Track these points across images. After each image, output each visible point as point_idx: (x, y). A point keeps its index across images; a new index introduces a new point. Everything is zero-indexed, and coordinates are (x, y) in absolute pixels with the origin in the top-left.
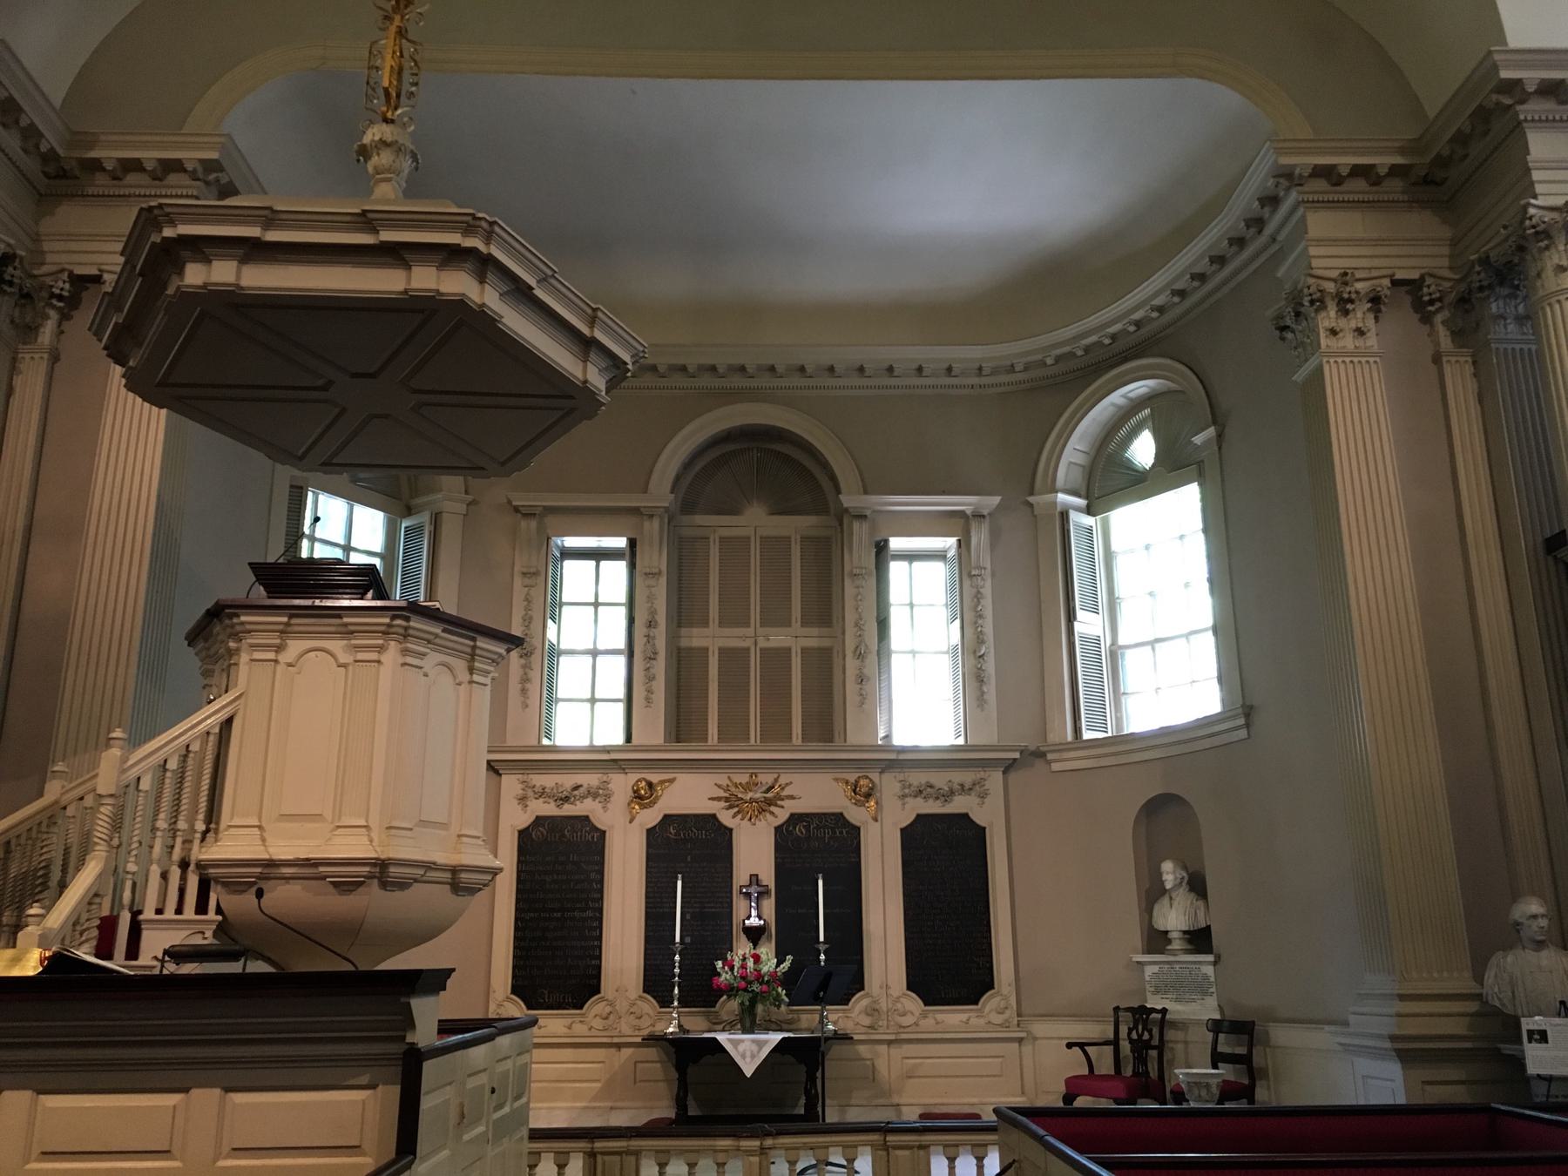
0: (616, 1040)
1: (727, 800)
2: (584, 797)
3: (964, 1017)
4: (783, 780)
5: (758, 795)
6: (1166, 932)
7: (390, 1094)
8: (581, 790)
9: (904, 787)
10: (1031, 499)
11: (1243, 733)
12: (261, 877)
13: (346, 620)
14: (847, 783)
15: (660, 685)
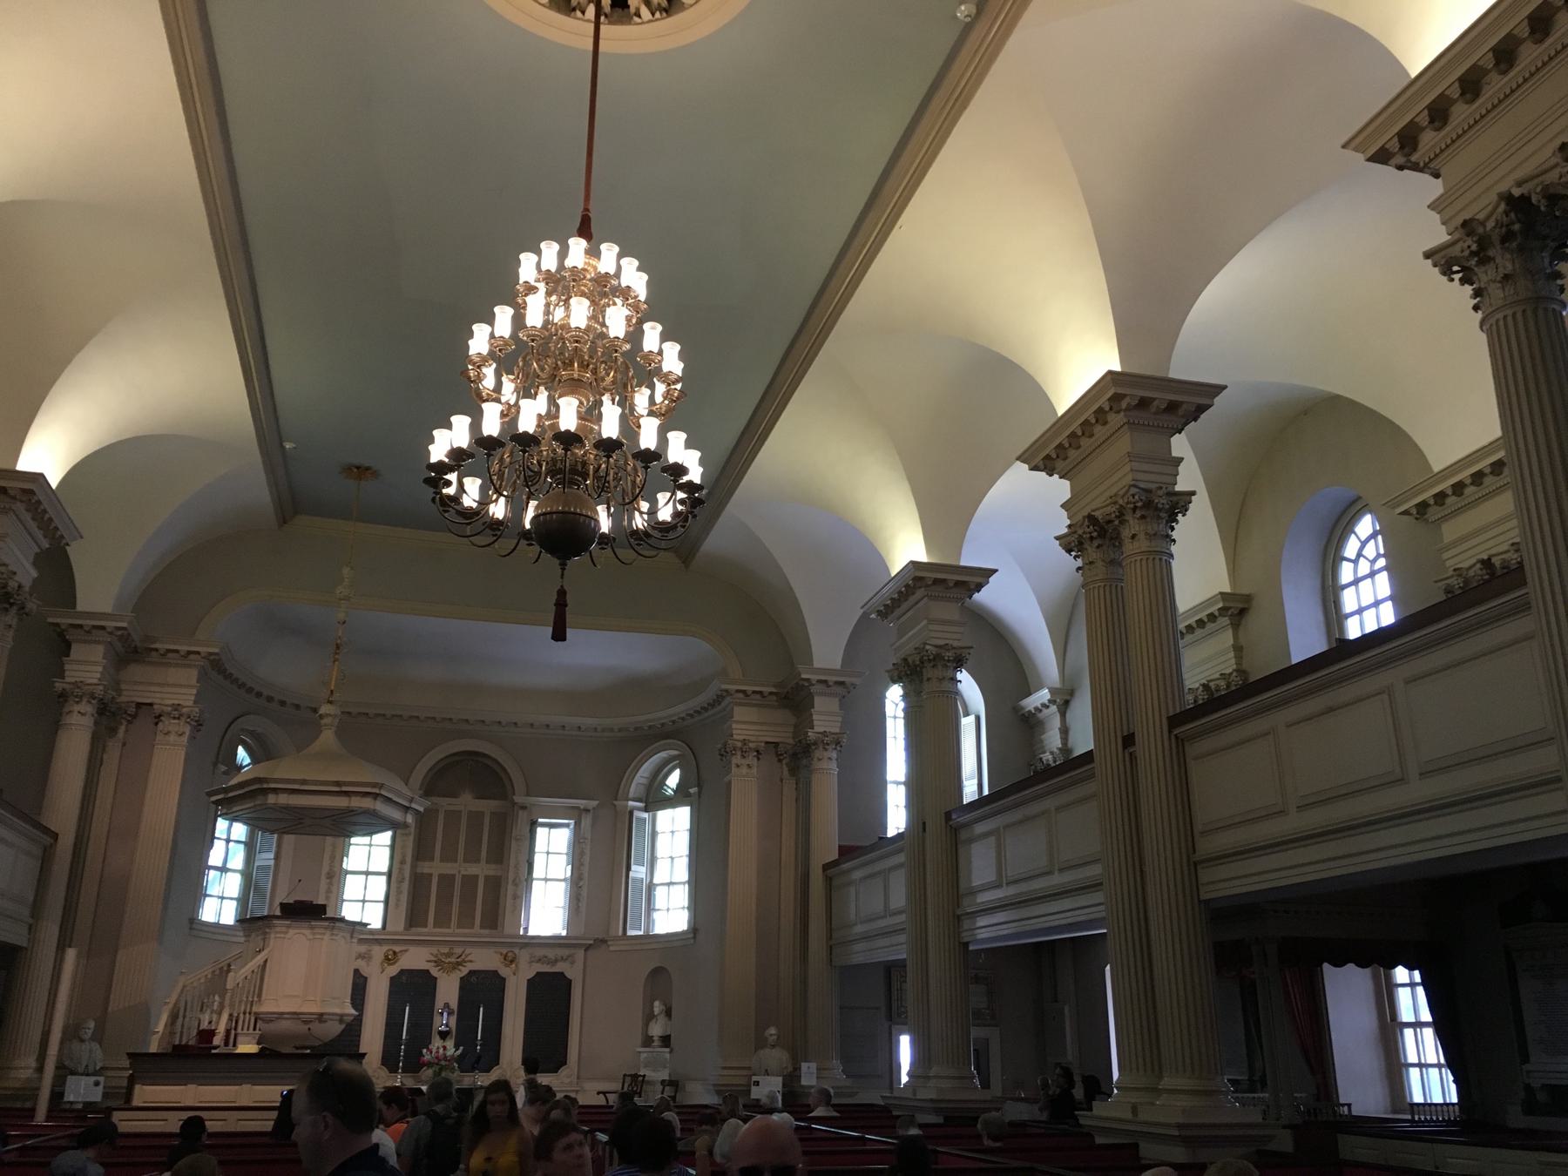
1: (435, 962)
4: (467, 951)
6: (652, 1037)
10: (615, 802)
11: (692, 941)
12: (277, 1018)
15: (404, 898)
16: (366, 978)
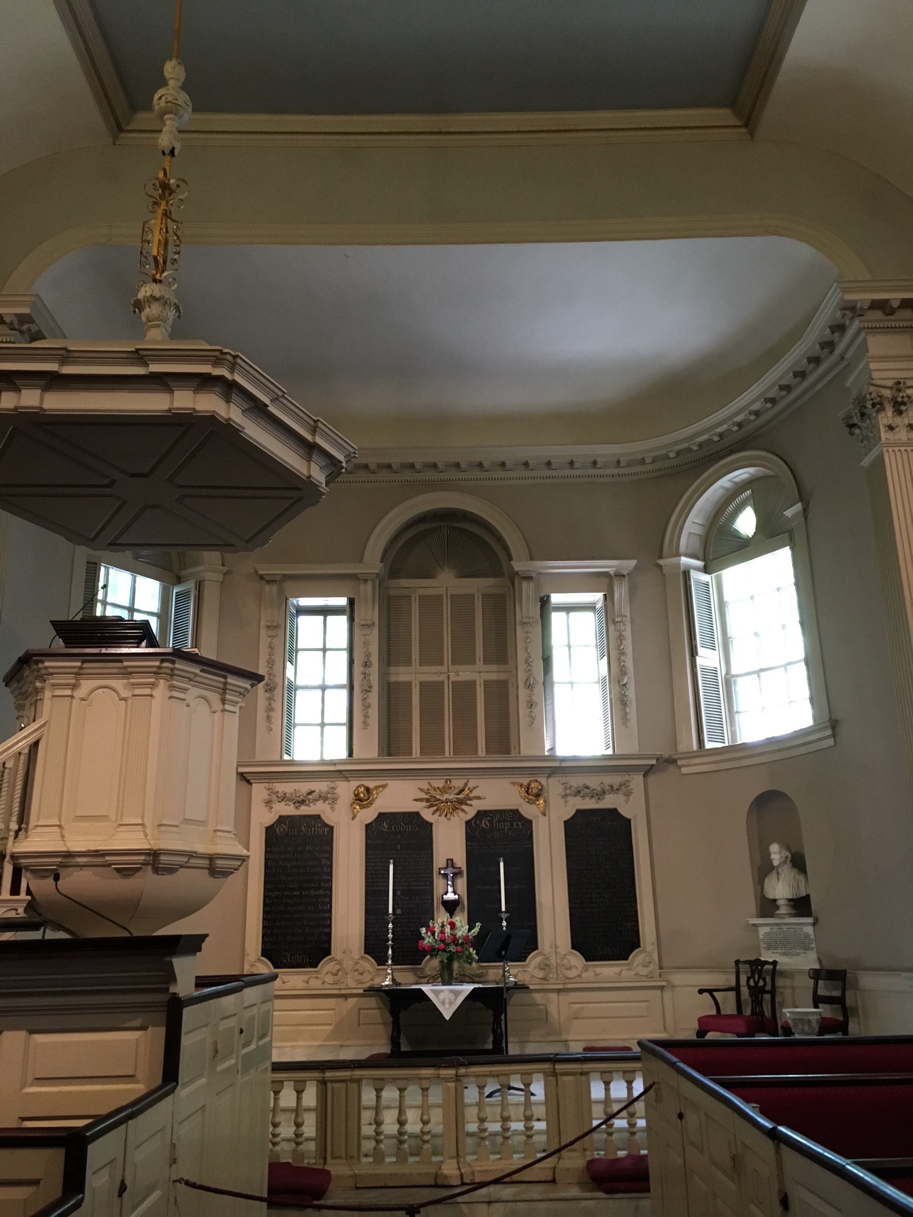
0: (343, 992)
1: (428, 800)
2: (316, 800)
3: (617, 969)
4: (471, 784)
5: (452, 797)
6: (775, 900)
7: (158, 1033)
8: (314, 794)
9: (566, 789)
10: (661, 562)
11: (831, 742)
12: (62, 866)
13: (126, 664)
14: (521, 786)
15: (374, 712)
16: (332, 828)
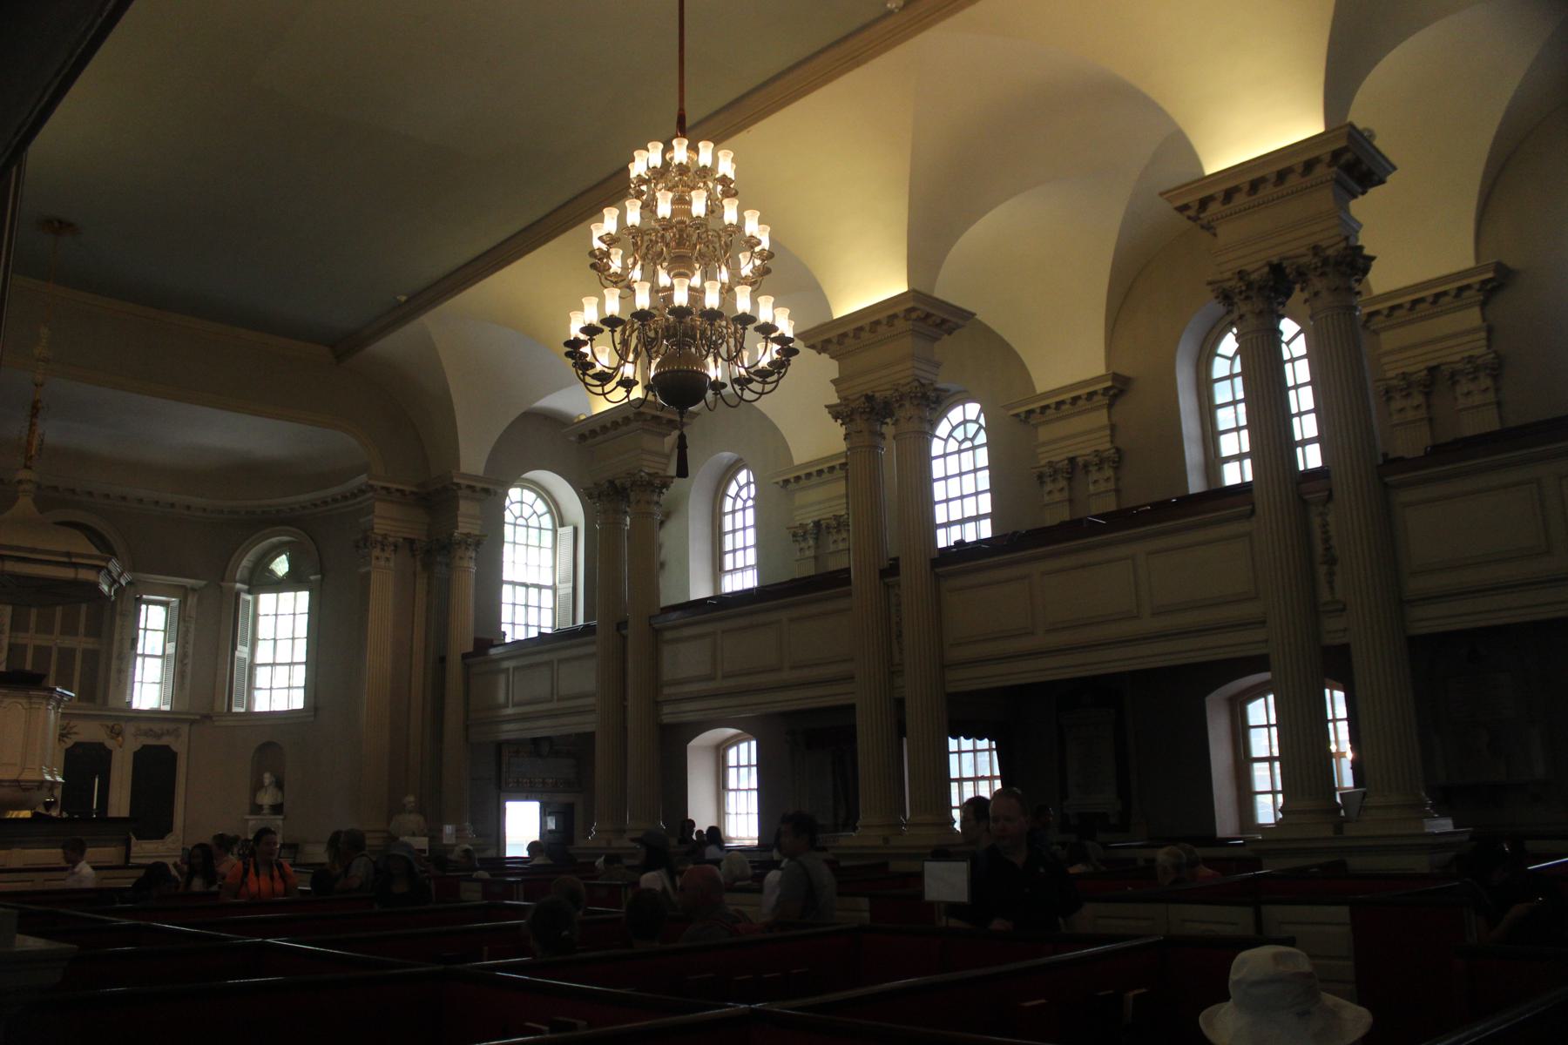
3: (156, 846)
4: (72, 724)
14: (108, 727)
